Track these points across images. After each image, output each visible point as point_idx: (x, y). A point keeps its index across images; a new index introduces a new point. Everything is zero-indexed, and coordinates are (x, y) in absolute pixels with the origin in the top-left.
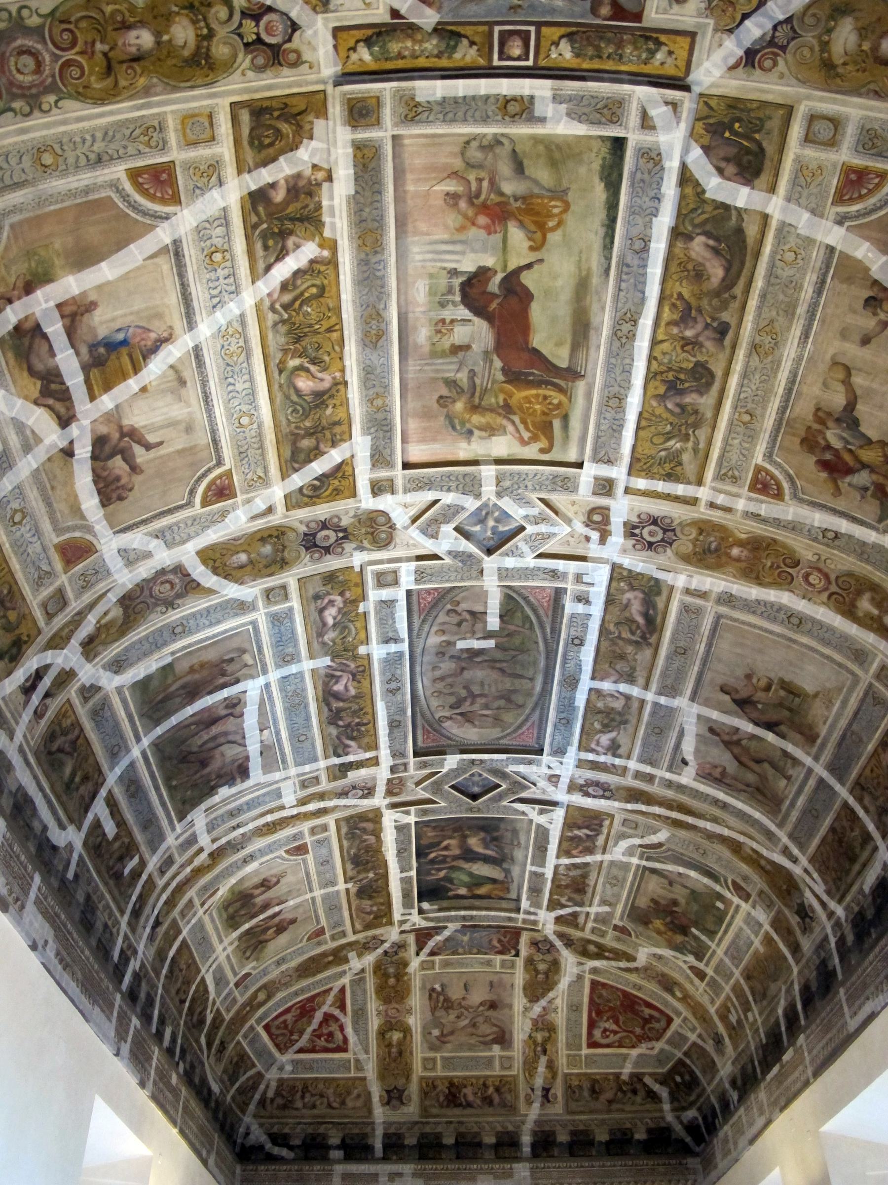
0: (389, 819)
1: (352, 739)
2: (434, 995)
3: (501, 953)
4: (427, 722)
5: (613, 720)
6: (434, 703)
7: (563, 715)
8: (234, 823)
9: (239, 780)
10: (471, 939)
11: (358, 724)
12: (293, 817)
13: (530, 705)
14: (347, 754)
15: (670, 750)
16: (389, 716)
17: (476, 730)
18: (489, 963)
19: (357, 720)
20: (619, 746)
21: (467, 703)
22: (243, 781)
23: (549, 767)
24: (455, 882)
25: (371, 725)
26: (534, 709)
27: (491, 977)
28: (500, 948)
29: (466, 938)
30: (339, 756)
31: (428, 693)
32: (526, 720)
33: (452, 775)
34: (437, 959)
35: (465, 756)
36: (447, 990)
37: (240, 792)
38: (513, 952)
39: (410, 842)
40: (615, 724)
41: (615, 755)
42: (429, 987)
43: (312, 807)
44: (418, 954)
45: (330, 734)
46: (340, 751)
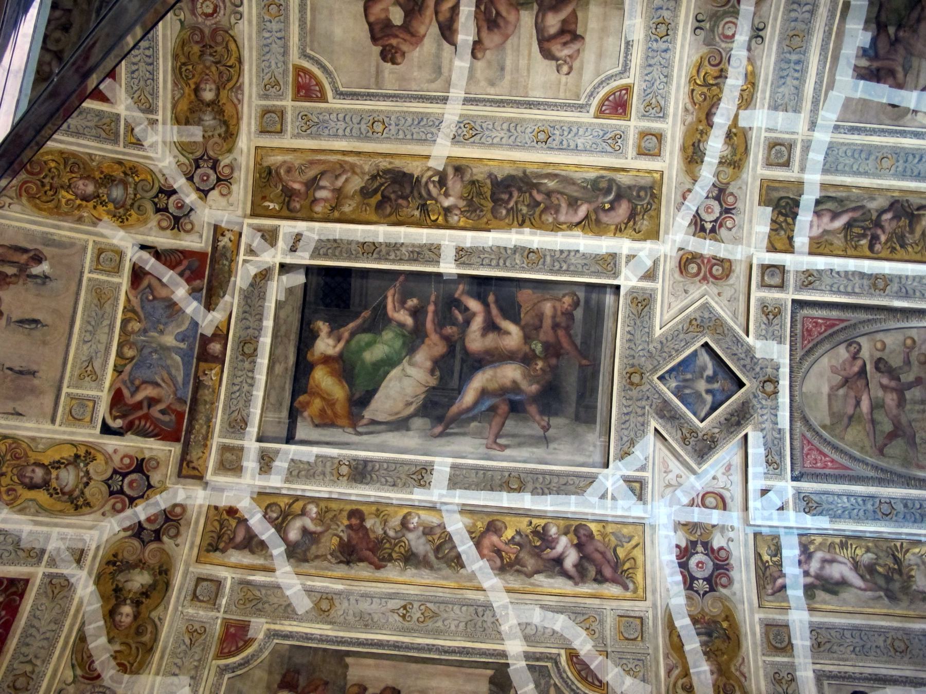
0: (646, 250)
1: (848, 226)
2: (24, 258)
3: (117, 398)
4: (854, 326)
5: (888, 579)
6: (891, 340)
7: (900, 507)
8: (773, 34)
9: (864, 63)
10: (165, 349)
11: (875, 239)
12: (709, 115)
13: (883, 463)
14: (817, 213)
15: (870, 671)
16: (900, 277)
17: (825, 390)
18: (89, 373)
19: (883, 238)
20: (834, 593)
21: (885, 381)
22: (856, 68)
23: (764, 492)
24: (365, 337)
25: (868, 253)
26: (876, 468)
27: (47, 375)
28: (131, 401)
29: (169, 340)
30: (818, 202)
31: (914, 333)
32: (853, 458)
33: (740, 352)
34: (124, 281)
35: (785, 371)
36: (30, 284)
37: (836, 58)
38: (118, 424)
39: (552, 271)
40: (881, 582)
41: (809, 590)
42: (47, 251)
43: (715, 146)
44: (143, 247)
45: (872, 199)
46: (830, 205)
